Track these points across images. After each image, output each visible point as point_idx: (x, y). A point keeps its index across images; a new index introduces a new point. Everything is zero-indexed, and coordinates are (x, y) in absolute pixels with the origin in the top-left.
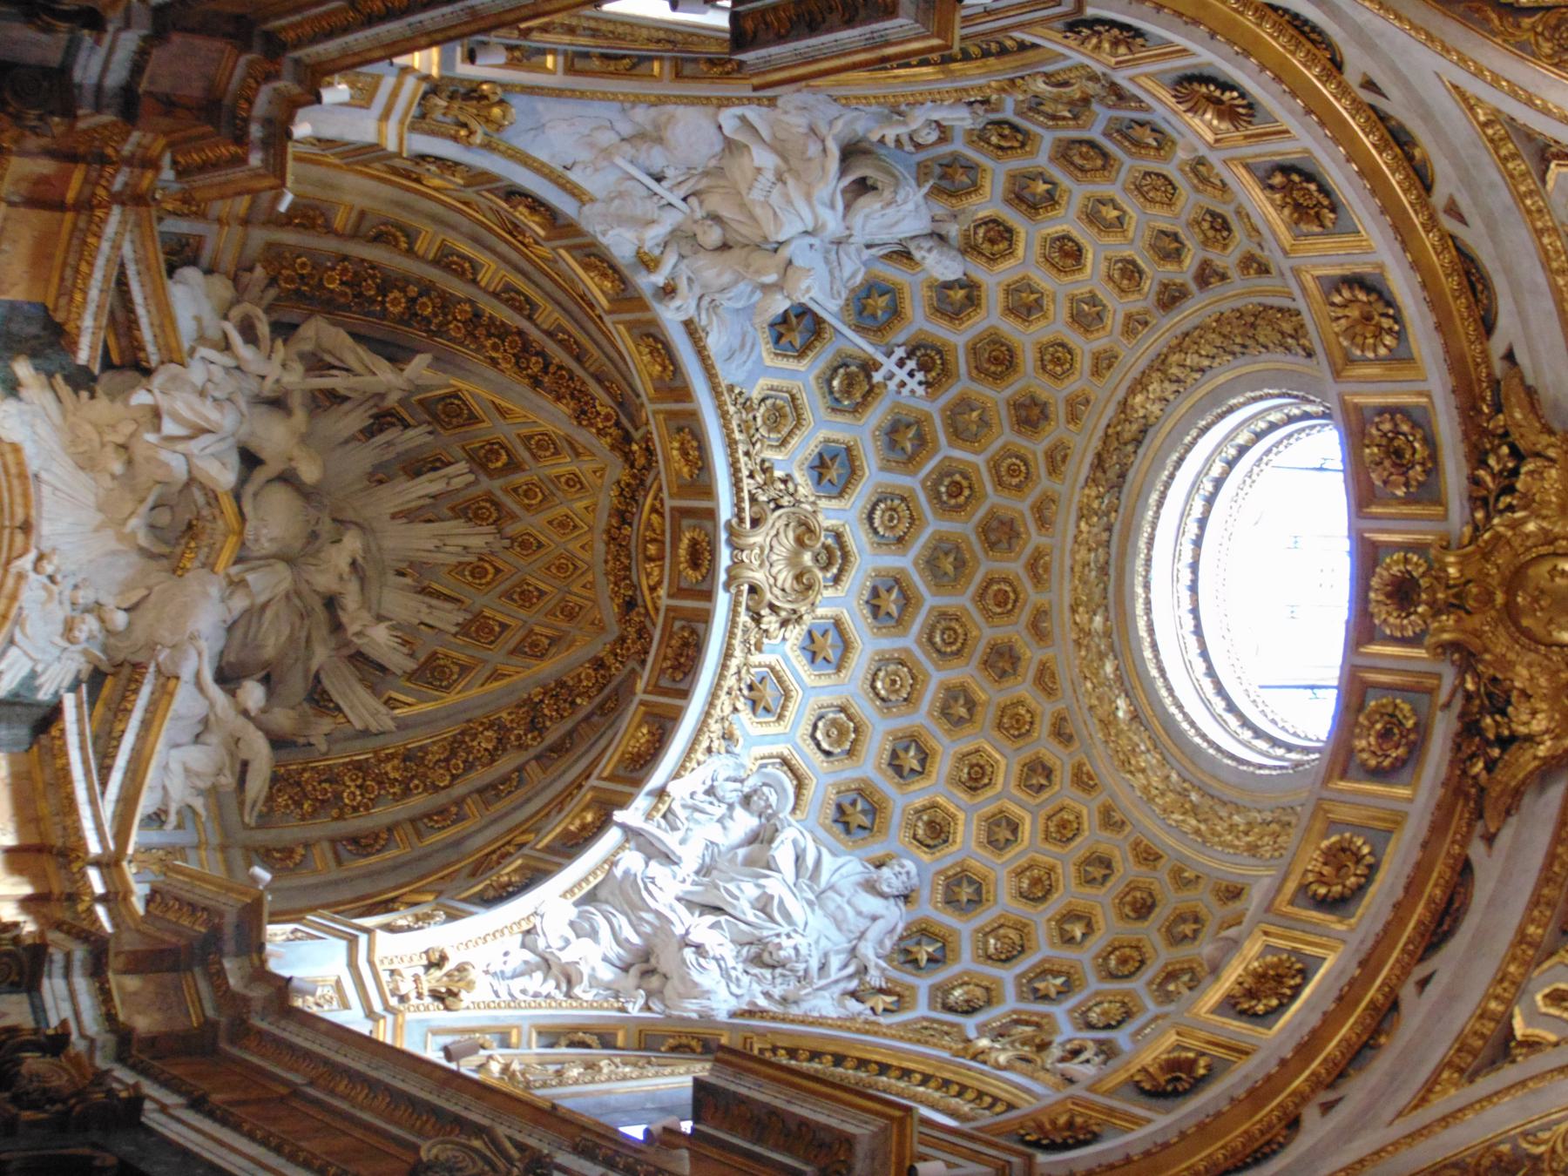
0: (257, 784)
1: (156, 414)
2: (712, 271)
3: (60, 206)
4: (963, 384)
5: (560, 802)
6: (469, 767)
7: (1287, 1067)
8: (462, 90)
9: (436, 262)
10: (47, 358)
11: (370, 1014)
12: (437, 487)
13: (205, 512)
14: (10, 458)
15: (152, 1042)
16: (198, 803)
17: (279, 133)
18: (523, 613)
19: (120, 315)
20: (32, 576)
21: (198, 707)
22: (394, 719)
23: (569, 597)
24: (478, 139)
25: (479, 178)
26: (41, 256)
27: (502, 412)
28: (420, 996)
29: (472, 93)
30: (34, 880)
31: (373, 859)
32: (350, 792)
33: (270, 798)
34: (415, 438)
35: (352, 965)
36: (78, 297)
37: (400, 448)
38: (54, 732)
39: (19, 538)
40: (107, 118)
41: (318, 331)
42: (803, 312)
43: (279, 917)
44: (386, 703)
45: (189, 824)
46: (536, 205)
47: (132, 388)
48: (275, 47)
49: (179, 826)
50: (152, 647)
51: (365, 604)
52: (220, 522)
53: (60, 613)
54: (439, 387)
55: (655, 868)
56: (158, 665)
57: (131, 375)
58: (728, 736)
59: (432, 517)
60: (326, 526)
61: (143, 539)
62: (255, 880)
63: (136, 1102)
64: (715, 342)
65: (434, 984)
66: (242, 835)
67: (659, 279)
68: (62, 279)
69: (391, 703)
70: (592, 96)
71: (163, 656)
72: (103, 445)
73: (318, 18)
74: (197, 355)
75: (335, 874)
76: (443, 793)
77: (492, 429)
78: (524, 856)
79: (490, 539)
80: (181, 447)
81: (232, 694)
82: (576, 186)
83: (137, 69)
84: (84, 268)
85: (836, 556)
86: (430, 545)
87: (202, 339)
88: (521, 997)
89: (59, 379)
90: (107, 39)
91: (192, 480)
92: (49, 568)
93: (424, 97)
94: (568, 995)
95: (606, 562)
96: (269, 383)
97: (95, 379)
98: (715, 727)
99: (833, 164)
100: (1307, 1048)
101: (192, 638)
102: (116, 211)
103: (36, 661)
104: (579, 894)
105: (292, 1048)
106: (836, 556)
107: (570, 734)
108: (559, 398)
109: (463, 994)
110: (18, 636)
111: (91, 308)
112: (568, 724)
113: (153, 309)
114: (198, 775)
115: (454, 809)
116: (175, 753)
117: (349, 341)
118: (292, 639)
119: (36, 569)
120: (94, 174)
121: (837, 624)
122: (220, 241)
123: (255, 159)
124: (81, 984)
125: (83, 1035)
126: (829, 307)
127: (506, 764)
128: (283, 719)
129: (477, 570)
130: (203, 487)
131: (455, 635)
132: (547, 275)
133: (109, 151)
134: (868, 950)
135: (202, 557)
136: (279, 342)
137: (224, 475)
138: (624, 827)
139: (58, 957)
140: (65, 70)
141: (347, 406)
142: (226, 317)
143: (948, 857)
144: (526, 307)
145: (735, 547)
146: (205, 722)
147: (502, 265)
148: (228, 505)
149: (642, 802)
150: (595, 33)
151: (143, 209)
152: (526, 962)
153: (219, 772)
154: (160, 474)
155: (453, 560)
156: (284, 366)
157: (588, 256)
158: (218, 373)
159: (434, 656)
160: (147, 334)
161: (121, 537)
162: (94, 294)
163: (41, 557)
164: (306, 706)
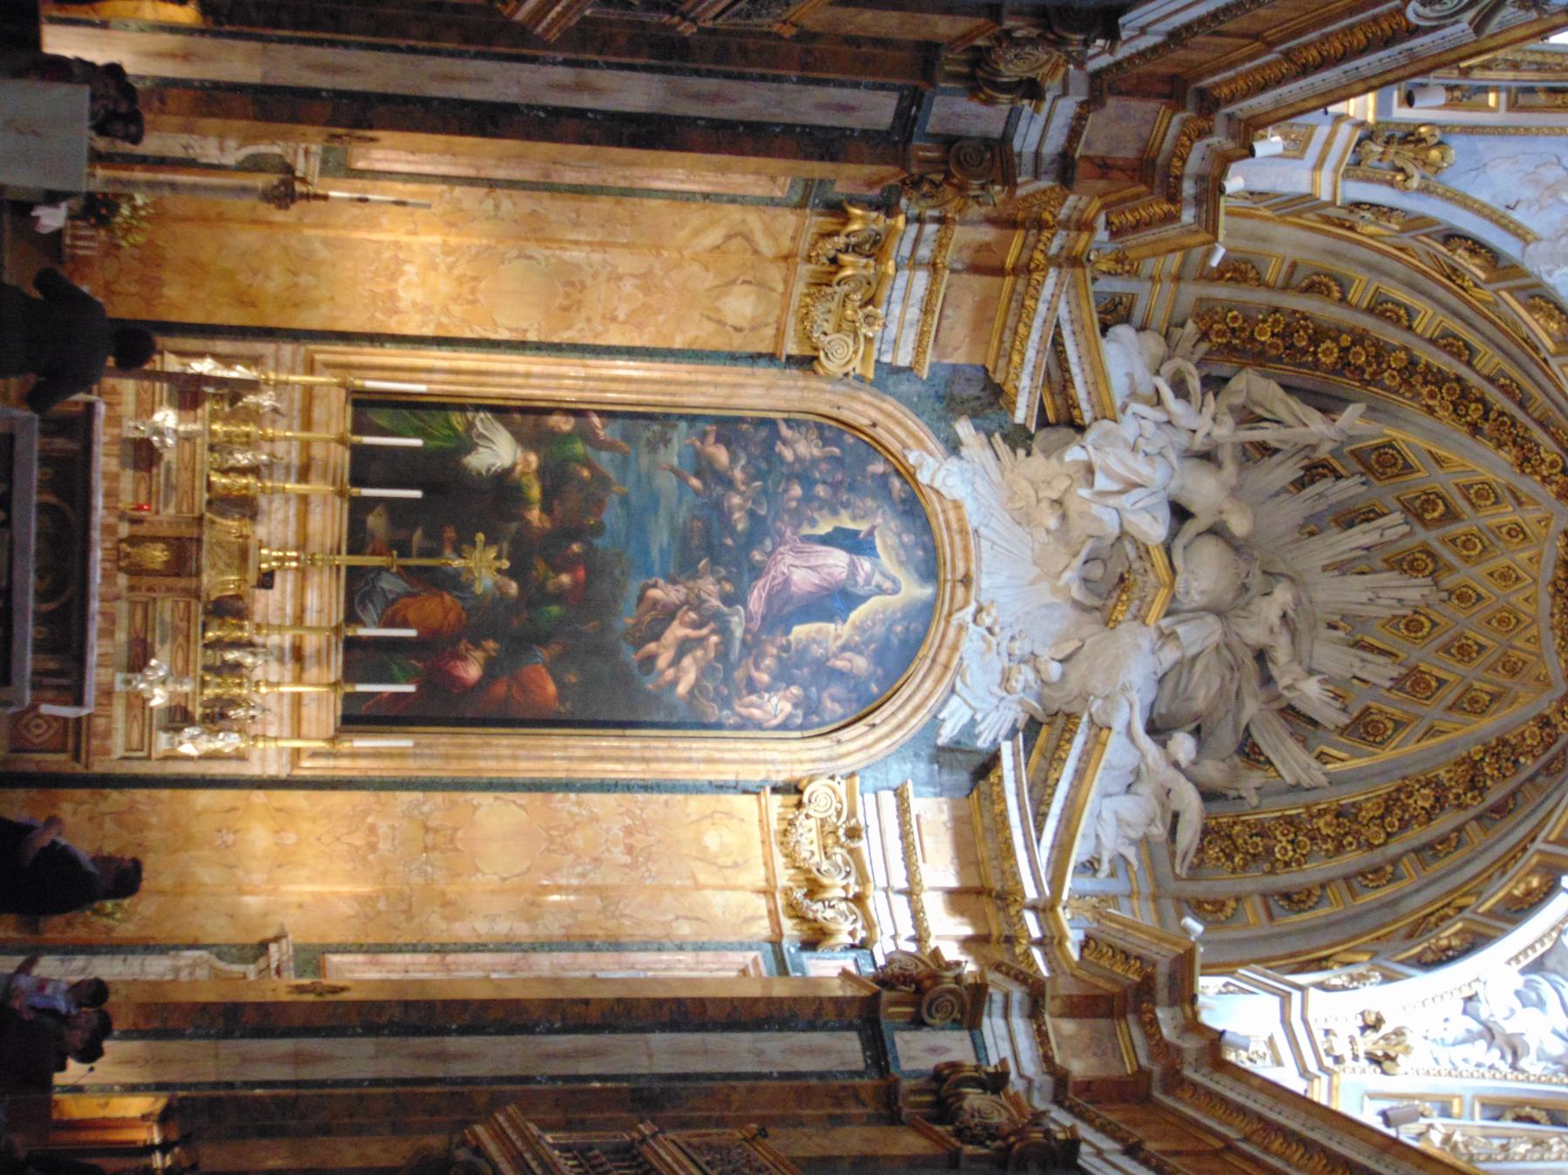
0: (1188, 835)
1: (1090, 469)
3: (999, 271)
5: (1504, 864)
6: (1404, 825)
8: (1399, 134)
9: (1370, 310)
10: (986, 418)
11: (1304, 1073)
12: (1366, 540)
13: (1136, 565)
14: (952, 515)
15: (1087, 1087)
16: (1131, 854)
17: (1211, 188)
18: (1461, 668)
19: (1056, 375)
20: (972, 626)
21: (1129, 758)
22: (1325, 774)
23: (1510, 652)
24: (1415, 183)
25: (1416, 223)
26: (982, 318)
27: (1439, 461)
28: (1356, 1058)
29: (1410, 137)
30: (974, 922)
31: (1305, 916)
32: (1281, 846)
33: (1201, 850)
34: (1348, 489)
36: (1016, 358)
37: (1332, 500)
38: (993, 778)
39: (960, 590)
40: (1045, 183)
41: (1249, 384)
43: (1211, 969)
44: (1318, 758)
45: (1121, 873)
46: (1476, 247)
47: (1067, 444)
48: (1208, 104)
49: (1112, 874)
50: (1084, 697)
51: (1296, 657)
52: (1151, 576)
53: (998, 664)
54: (1373, 438)
56: (1091, 715)
57: (1066, 432)
59: (1364, 568)
60: (1256, 580)
61: (1077, 592)
62: (1186, 931)
63: (1073, 1144)
65: (1370, 1047)
66: (1173, 886)
68: (1001, 341)
69: (1321, 757)
70: (1539, 132)
71: (1096, 706)
72: (1038, 501)
73: (1250, 72)
74: (1129, 411)
75: (1266, 928)
76: (1378, 852)
77: (1426, 478)
78: (1463, 919)
79: (1426, 591)
80: (1112, 501)
81: (1164, 745)
82: (1519, 226)
83: (1074, 134)
84: (1022, 329)
86: (1364, 597)
87: (1134, 395)
88: (1462, 1066)
89: (997, 436)
90: (1045, 107)
91: (1123, 535)
92: (988, 621)
93: (1359, 144)
94: (1514, 1067)
95: (1552, 615)
96: (1200, 436)
97: (1031, 437)
101: (1124, 689)
102: (1052, 274)
103: (975, 710)
104: (1524, 962)
105: (1224, 1100)
107: (1513, 794)
108: (1500, 445)
109: (1401, 1059)
110: (959, 686)
111: (1029, 368)
112: (1510, 785)
113: (1087, 368)
114: (1129, 825)
115: (1389, 869)
116: (1107, 801)
117: (1280, 392)
118: (1221, 691)
119: (975, 621)
120: (1031, 240)
122: (1151, 299)
123: (1188, 216)
124: (1020, 1024)
125: (1021, 1076)
127: (1444, 823)
128: (1213, 772)
130: (1134, 540)
131: (1389, 690)
132: (1486, 317)
133: (1047, 216)
135: (1133, 610)
136: (1210, 396)
137: (1154, 528)
139: (998, 997)
140: (1006, 139)
141: (1278, 458)
142: (1157, 373)
144: (1465, 353)
146: (1137, 773)
147: (1440, 310)
148: (1159, 558)
150: (1540, 67)
151: (1078, 271)
152: (1469, 1031)
153: (1152, 822)
154: (1093, 529)
155: (1387, 613)
156: (1214, 419)
157: (1533, 297)
158: (1149, 428)
159: (1367, 711)
160: (1080, 392)
161: (1055, 591)
162: (1031, 354)
163: (980, 610)
164: (1237, 760)
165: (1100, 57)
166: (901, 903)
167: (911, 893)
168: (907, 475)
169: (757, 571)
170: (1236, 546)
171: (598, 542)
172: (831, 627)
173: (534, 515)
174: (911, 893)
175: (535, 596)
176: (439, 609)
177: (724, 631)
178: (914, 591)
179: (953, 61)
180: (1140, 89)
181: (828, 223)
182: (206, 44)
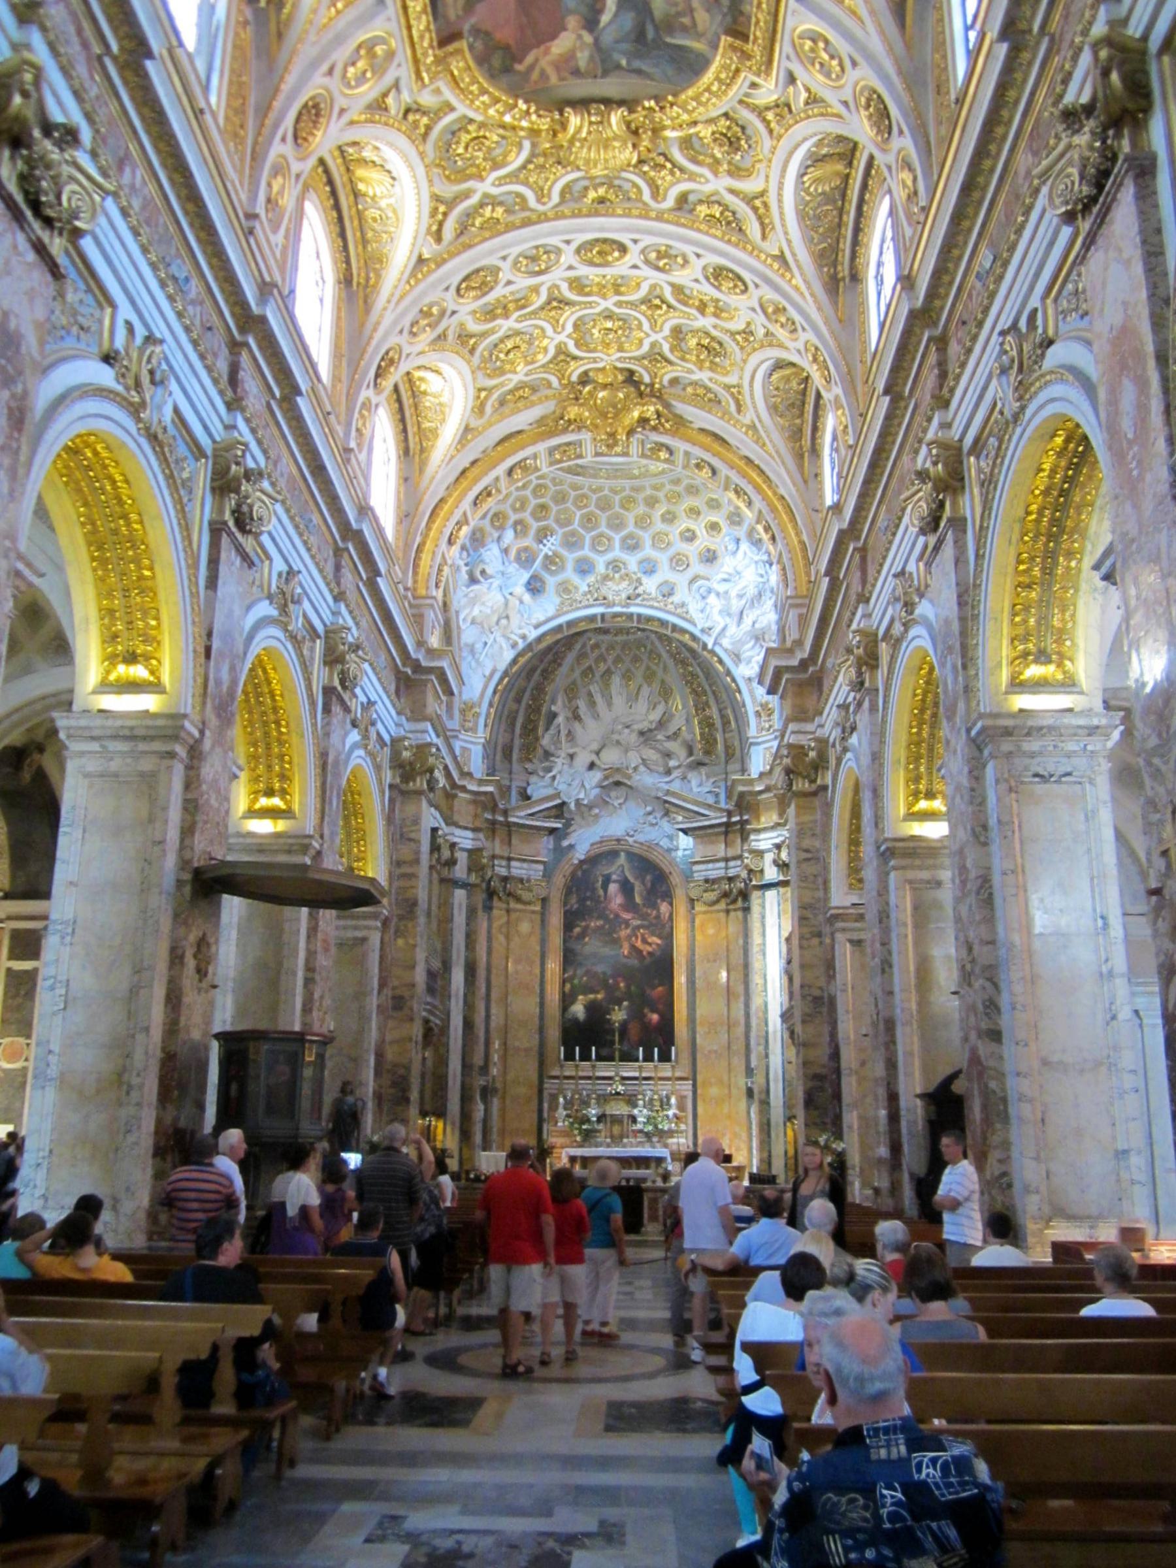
4: (551, 522)
7: (765, 498)
25: (491, 705)
35: (758, 744)
42: (529, 583)
53: (648, 828)
55: (728, 634)
58: (683, 605)
64: (542, 618)
67: (520, 641)
71: (660, 794)
83: (466, 828)
87: (551, 785)
90: (456, 840)
98: (679, 611)
99: (475, 587)
106: (615, 565)
121: (641, 562)
123: (490, 789)
124: (762, 836)
126: (526, 576)
129: (627, 676)
134: (757, 558)
138: (715, 643)
140: (469, 851)
143: (723, 524)
144: (532, 671)
145: (614, 605)
149: (705, 638)
165: (445, 829)
166: (732, 864)
167: (727, 860)
168: (582, 862)
169: (617, 916)
171: (609, 972)
172: (637, 889)
173: (600, 996)
174: (727, 860)
175: (628, 995)
176: (634, 1031)
177: (638, 927)
179: (445, 872)
180: (451, 808)
181: (495, 898)
182: (449, 1116)
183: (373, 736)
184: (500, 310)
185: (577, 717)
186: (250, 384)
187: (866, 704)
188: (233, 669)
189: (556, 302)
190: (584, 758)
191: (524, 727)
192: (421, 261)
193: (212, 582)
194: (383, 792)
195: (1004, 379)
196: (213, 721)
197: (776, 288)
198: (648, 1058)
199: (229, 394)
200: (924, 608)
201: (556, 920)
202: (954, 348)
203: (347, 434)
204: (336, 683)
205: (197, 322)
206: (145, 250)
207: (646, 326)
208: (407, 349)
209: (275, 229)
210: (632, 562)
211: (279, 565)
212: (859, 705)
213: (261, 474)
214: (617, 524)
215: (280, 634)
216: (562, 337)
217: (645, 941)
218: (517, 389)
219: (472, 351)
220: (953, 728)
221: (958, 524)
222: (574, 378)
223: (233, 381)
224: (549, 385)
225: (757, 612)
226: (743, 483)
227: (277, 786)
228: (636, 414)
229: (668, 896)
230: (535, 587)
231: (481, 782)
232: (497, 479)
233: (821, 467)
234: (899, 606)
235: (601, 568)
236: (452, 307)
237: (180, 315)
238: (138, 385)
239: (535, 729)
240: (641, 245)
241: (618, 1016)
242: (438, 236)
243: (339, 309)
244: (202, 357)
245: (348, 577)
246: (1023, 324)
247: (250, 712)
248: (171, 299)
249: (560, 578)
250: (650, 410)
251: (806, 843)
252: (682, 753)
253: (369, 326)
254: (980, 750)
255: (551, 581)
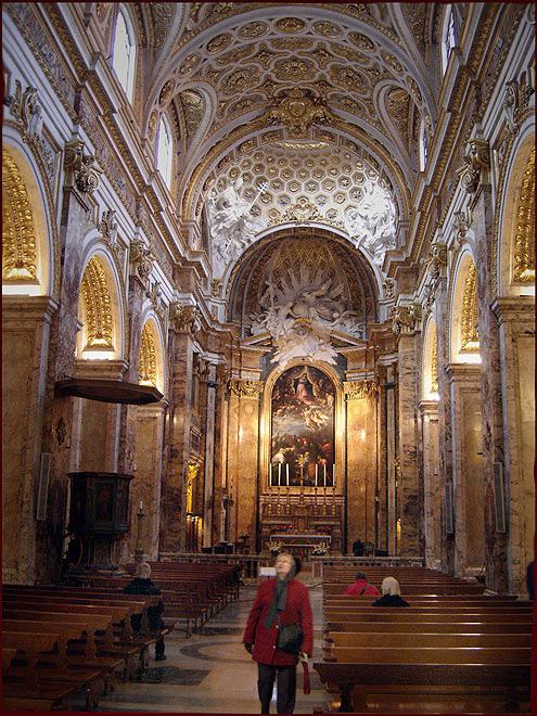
2: (245, 234)
25: (229, 281)
64: (259, 231)
85: (303, 199)
98: (339, 226)
100: (383, 159)
124: (387, 357)
127: (350, 261)
137: (292, 321)
149: (354, 242)
169: (303, 403)
170: (295, 304)
175: (308, 448)
177: (315, 410)
178: (306, 370)
180: (206, 341)
183: (159, 302)
184: (233, 57)
185: (281, 288)
186: (87, 108)
187: (440, 287)
188: (76, 268)
189: (264, 52)
190: (284, 311)
191: (249, 293)
192: (186, 31)
193: (65, 221)
194: (164, 334)
195: (509, 109)
196: (66, 300)
197: (390, 47)
198: (321, 484)
199: (75, 115)
200: (470, 234)
201: (267, 405)
202: (484, 88)
203: (143, 130)
204: (137, 273)
205: (57, 77)
206: (27, 41)
207: (317, 66)
208: (178, 81)
209: (102, 19)
210: (312, 198)
211: (103, 208)
212: (436, 286)
213: (92, 159)
214: (304, 174)
215: (105, 248)
216: (268, 72)
217: (318, 417)
218: (242, 101)
219: (216, 81)
220: (483, 304)
221: (487, 188)
222: (275, 95)
223: (77, 107)
224: (261, 99)
225: (384, 227)
226: (374, 155)
227: (103, 333)
228: (312, 115)
229: (333, 392)
230: (255, 211)
231: (223, 326)
232: (231, 152)
233: (418, 146)
234: (457, 231)
235: (294, 202)
236: (204, 56)
237: (47, 74)
238: (23, 115)
239: (256, 294)
240: (313, 22)
241: (302, 461)
242: (196, 20)
243: (139, 61)
244: (59, 96)
245: (143, 212)
246: (518, 79)
247: (88, 291)
248: (41, 65)
249: (271, 206)
250: (320, 112)
251: (408, 364)
252: (341, 310)
253: (156, 68)
254: (497, 318)
255: (265, 209)
